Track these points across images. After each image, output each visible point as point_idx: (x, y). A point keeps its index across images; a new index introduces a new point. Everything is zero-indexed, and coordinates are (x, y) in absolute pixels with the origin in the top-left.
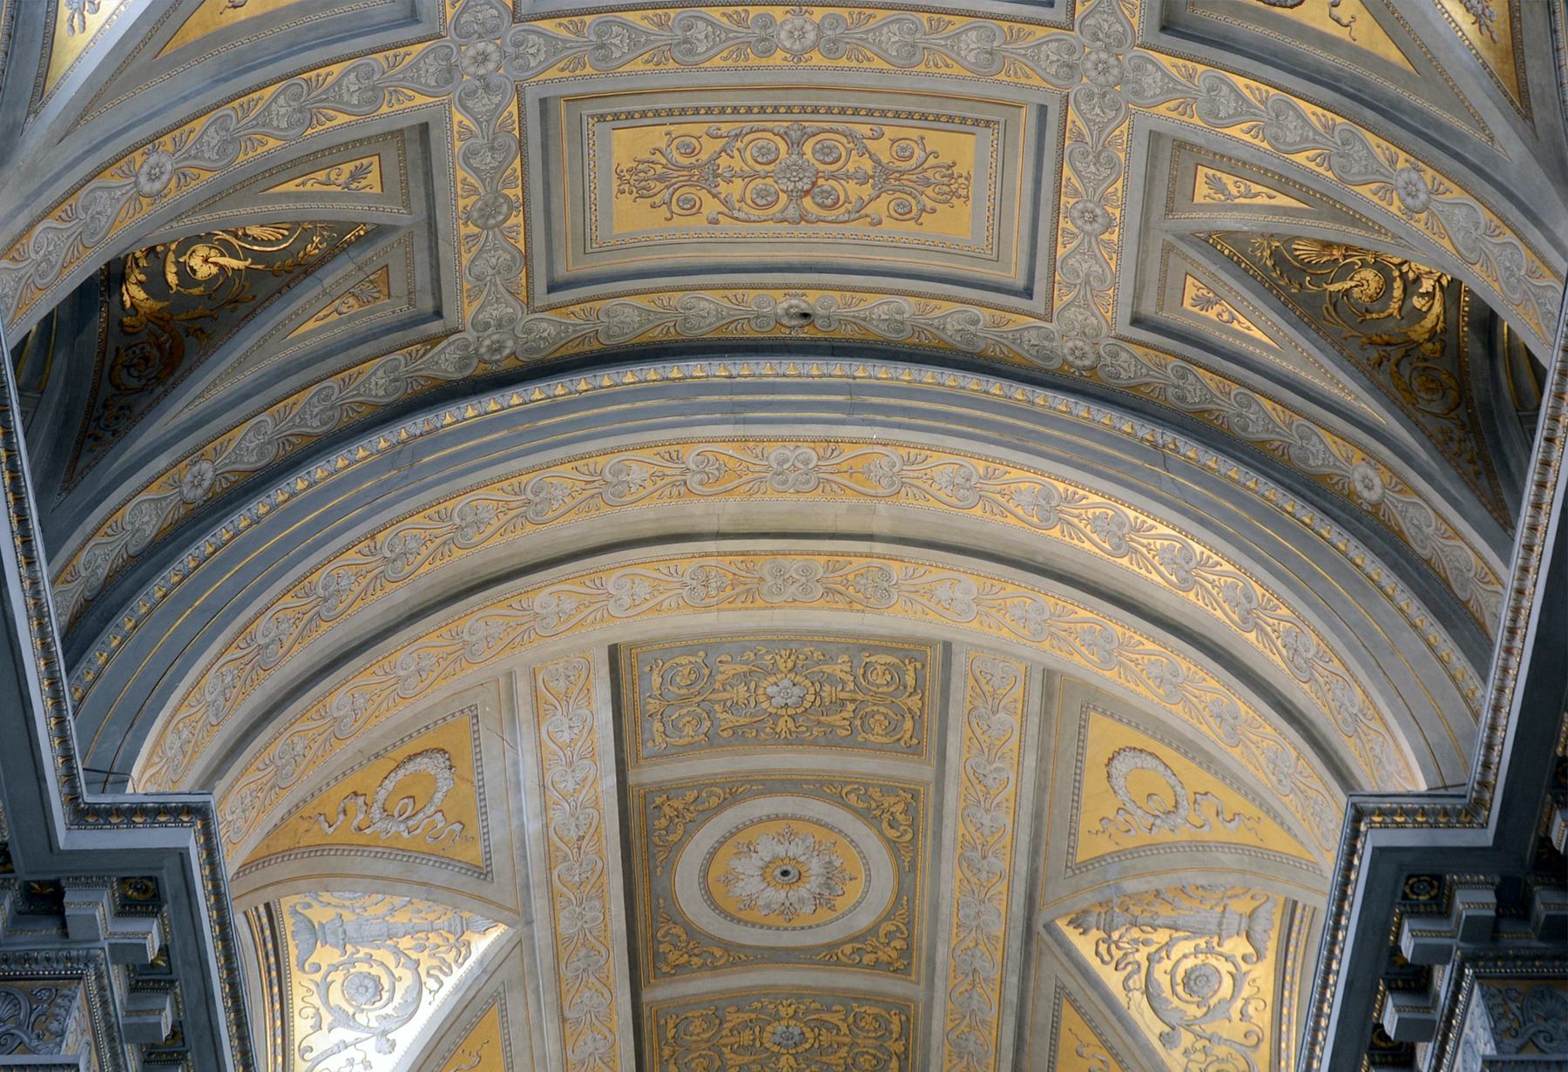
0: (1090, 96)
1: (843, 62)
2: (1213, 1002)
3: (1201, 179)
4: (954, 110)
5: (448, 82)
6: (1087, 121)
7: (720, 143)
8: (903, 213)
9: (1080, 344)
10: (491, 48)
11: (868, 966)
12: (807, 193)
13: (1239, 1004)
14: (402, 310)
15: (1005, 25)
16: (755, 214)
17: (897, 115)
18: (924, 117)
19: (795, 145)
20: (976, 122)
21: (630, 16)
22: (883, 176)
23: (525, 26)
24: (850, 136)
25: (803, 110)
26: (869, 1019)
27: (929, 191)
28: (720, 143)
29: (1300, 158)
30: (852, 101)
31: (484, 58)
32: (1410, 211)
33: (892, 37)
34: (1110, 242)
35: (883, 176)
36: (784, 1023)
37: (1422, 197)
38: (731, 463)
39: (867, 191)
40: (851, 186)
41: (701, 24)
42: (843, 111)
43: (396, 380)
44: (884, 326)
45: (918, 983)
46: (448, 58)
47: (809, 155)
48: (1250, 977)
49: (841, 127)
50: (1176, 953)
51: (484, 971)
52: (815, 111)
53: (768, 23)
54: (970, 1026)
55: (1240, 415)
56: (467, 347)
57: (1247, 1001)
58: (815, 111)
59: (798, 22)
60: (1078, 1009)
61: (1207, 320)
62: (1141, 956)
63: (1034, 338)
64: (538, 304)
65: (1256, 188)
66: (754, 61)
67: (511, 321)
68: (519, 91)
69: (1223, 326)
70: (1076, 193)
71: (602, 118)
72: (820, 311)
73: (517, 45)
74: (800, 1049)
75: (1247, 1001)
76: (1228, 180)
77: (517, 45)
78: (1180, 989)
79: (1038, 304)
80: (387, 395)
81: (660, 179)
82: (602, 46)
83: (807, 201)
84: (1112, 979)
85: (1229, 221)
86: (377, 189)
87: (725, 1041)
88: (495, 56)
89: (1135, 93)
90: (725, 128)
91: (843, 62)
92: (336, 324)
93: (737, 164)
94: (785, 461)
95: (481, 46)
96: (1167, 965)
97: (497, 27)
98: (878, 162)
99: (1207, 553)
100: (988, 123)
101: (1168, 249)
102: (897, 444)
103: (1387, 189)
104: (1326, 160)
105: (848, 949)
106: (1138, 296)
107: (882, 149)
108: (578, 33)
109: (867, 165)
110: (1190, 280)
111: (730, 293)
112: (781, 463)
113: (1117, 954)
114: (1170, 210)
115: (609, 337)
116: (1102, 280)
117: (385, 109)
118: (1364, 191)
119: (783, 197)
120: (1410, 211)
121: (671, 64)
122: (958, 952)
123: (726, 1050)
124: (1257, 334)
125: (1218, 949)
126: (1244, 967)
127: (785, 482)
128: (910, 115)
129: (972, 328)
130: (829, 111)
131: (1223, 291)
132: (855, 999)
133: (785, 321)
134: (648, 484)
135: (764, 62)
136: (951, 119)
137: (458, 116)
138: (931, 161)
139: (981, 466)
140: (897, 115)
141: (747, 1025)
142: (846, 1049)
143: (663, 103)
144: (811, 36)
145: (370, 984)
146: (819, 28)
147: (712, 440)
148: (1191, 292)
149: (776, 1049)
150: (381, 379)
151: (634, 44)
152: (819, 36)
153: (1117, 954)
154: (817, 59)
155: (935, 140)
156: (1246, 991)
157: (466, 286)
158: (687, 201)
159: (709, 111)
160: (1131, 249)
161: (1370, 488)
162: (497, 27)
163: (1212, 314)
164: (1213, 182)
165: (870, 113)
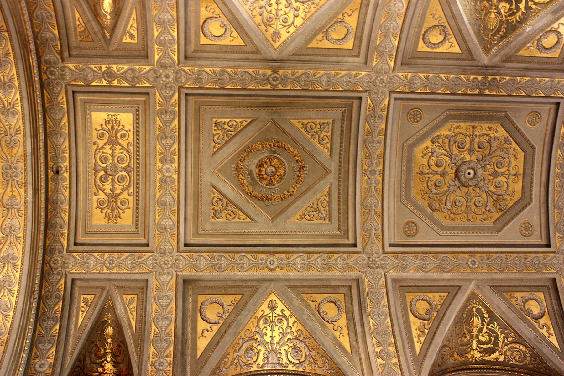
0: (155, 260)
1: (158, 184)
3: (132, 296)
4: (141, 218)
5: (161, 66)
6: (146, 259)
7: (126, 146)
8: (100, 203)
9: (60, 262)
10: (170, 79)
12: (106, 173)
14: (74, 43)
15: (176, 232)
16: (98, 157)
17: (137, 200)
18: (137, 209)
19: (125, 169)
20: (137, 225)
21: (176, 122)
22: (114, 196)
23: (177, 90)
24: (129, 186)
25: (138, 172)
27: (109, 211)
28: (126, 146)
29: (154, 327)
30: (141, 186)
31: (167, 77)
32: (153, 365)
33: (168, 199)
34: (103, 269)
35: (114, 196)
37: (161, 368)
38: (14, 151)
39: (108, 191)
40: (110, 187)
41: (172, 142)
42: (138, 184)
43: (47, 40)
44: (55, 198)
46: (170, 67)
47: (120, 173)
49: (132, 183)
52: (138, 175)
53: (172, 161)
55: (48, 318)
56: (55, 64)
58: (138, 175)
59: (172, 171)
61: (79, 303)
63: (58, 246)
64: (69, 87)
65: (134, 314)
66: (158, 157)
67: (63, 79)
68: (154, 87)
69: (79, 309)
70: (119, 258)
71: (138, 110)
72: (60, 177)
73: (170, 87)
76: (134, 305)
77: (170, 87)
79: (72, 247)
80: (41, 36)
81: (112, 127)
82: (166, 112)
83: (102, 173)
85: (119, 307)
86: (124, 41)
88: (167, 80)
89: (160, 273)
90: (131, 148)
91: (158, 184)
92: (74, 22)
93: (117, 152)
94: (16, 169)
95: (172, 77)
97: (177, 82)
98: (119, 194)
99: (11, 317)
100: (137, 228)
101: (103, 288)
102: (26, 207)
103: (155, 356)
104: (156, 335)
106: (82, 280)
107: (124, 196)
108: (172, 105)
109: (118, 191)
110: (93, 296)
111: (67, 148)
112: (15, 168)
114: (118, 287)
115: (50, 109)
116: (88, 268)
117: (156, 46)
118: (152, 349)
119: (104, 165)
120: (153, 365)
121: (158, 133)
124: (80, 320)
127: (6, 169)
128: (138, 204)
129: (58, 226)
130: (138, 180)
131: (93, 307)
133: (55, 166)
134: (7, 123)
135: (158, 160)
136: (137, 217)
137: (148, 68)
138: (121, 211)
139: (21, 235)
140: (137, 200)
143: (141, 130)
144: (167, 174)
146: (170, 177)
147: (25, 145)
148: (89, 297)
150: (49, 35)
151: (166, 122)
152: (167, 177)
154: (159, 176)
155: (129, 212)
157: (81, 66)
158: (103, 136)
159: (138, 143)
160: (102, 276)
161: (40, 366)
162: (177, 82)
163: (82, 304)
164: (132, 300)
165: (138, 192)
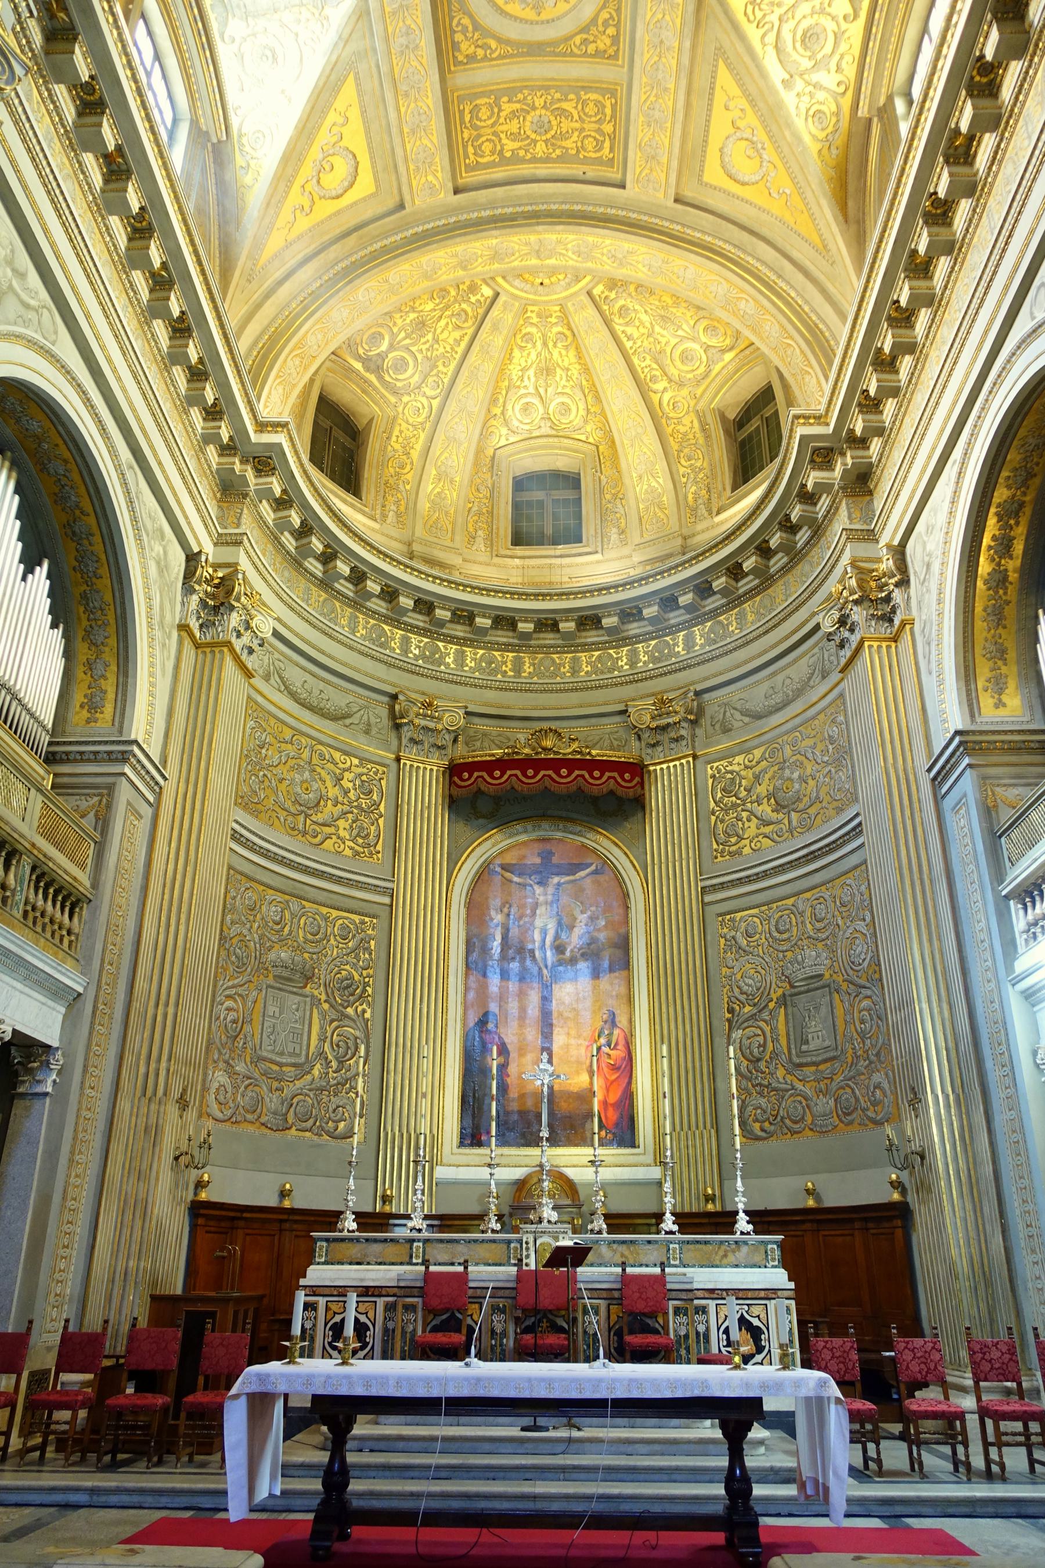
2: (819, 56)
11: (592, 56)
13: (836, 57)
26: (591, 105)
36: (538, 112)
45: (623, 67)
48: (846, 35)
50: (799, 13)
51: (340, 38)
54: (656, 96)
57: (842, 56)
60: (728, 66)
62: (774, 18)
74: (549, 136)
75: (842, 56)
78: (798, 45)
84: (753, 34)
87: (501, 128)
96: (791, 24)
105: (578, 40)
113: (759, 14)
122: (651, 26)
123: (503, 136)
125: (828, 10)
126: (844, 26)
132: (583, 88)
141: (514, 114)
142: (576, 134)
145: (269, 54)
149: (533, 136)
153: (759, 14)
156: (843, 47)
